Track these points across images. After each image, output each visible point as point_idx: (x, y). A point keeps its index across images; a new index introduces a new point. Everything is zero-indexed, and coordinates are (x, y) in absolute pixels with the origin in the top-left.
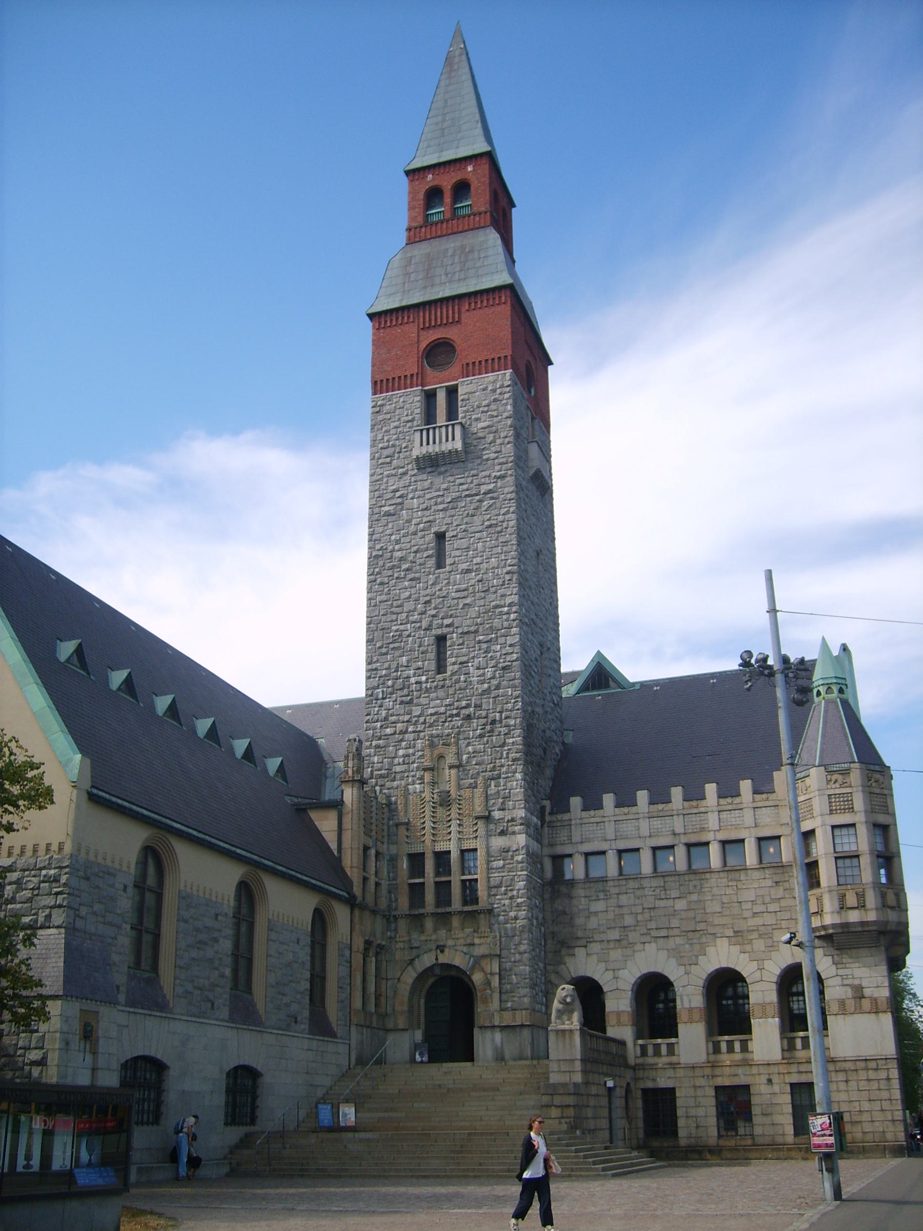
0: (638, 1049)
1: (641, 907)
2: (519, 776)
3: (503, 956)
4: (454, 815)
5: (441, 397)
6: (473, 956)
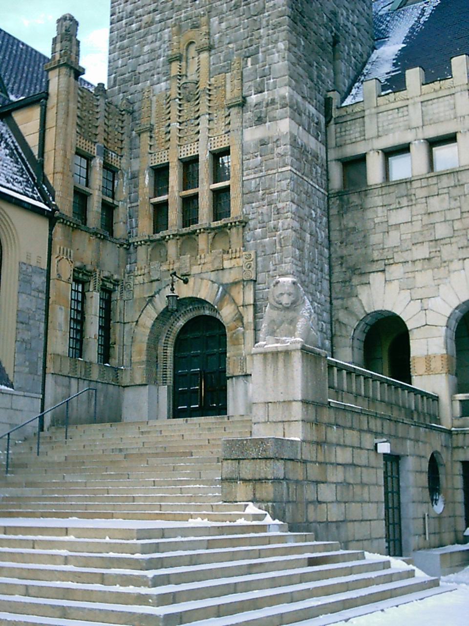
0: (457, 406)
1: (459, 210)
2: (281, 46)
3: (259, 280)
4: (203, 108)
6: (222, 284)
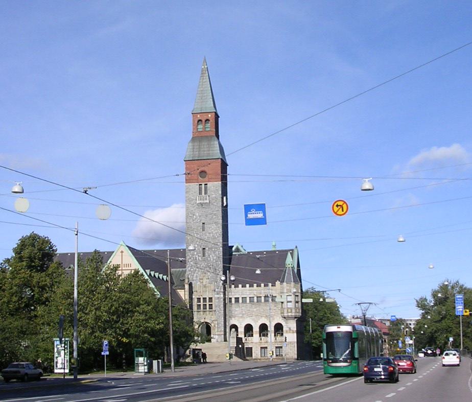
5: (203, 186)
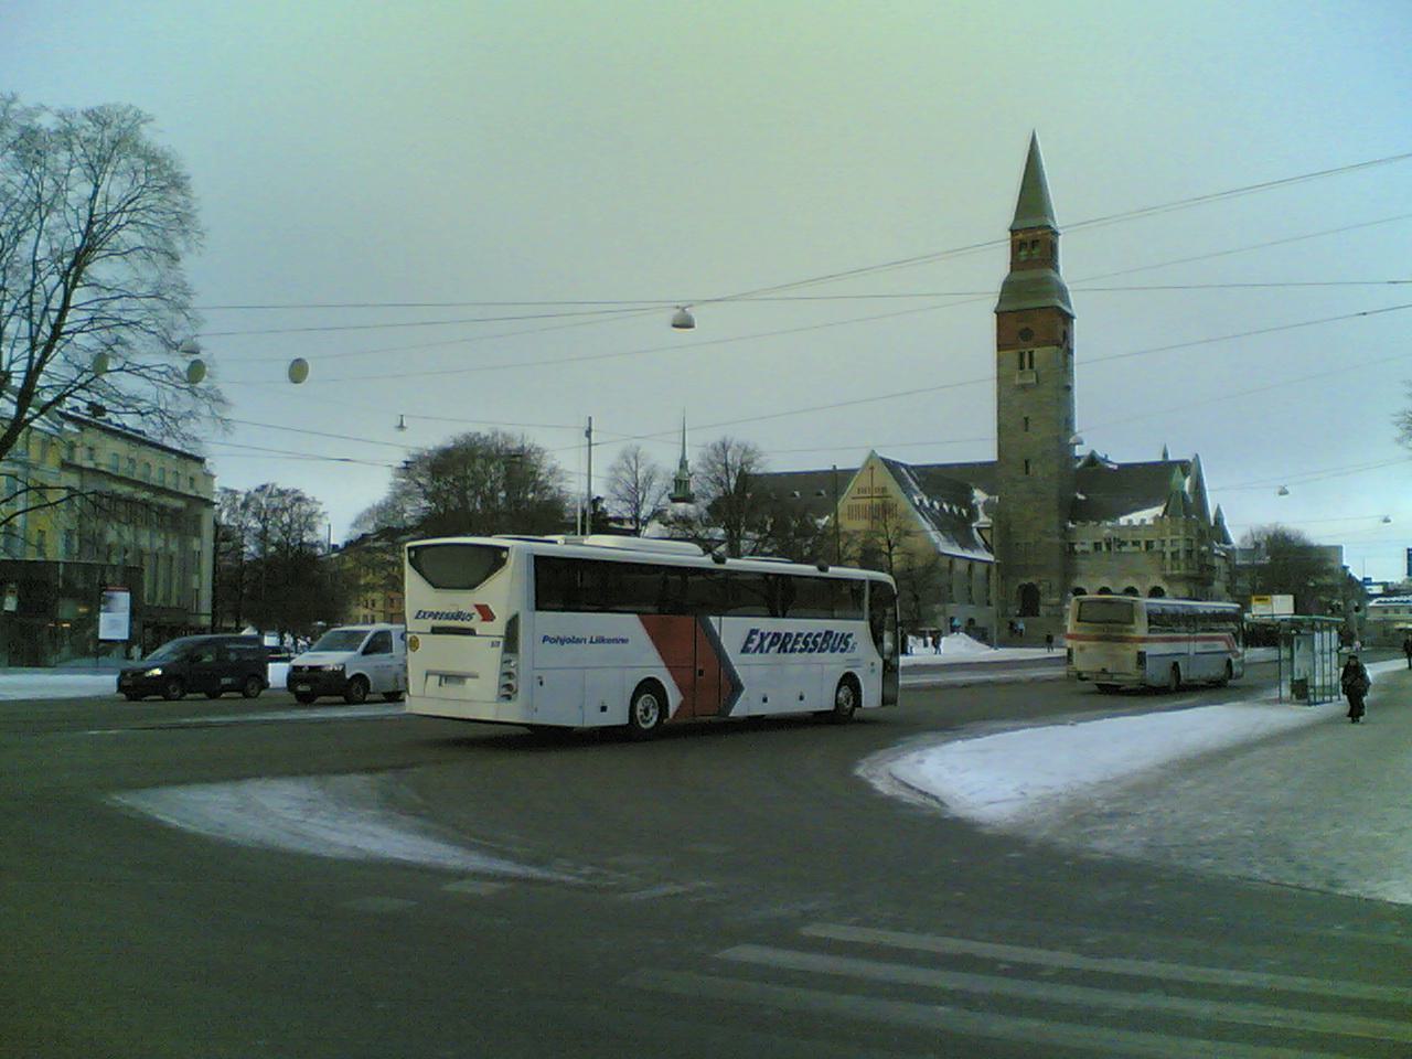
5: (1027, 355)
